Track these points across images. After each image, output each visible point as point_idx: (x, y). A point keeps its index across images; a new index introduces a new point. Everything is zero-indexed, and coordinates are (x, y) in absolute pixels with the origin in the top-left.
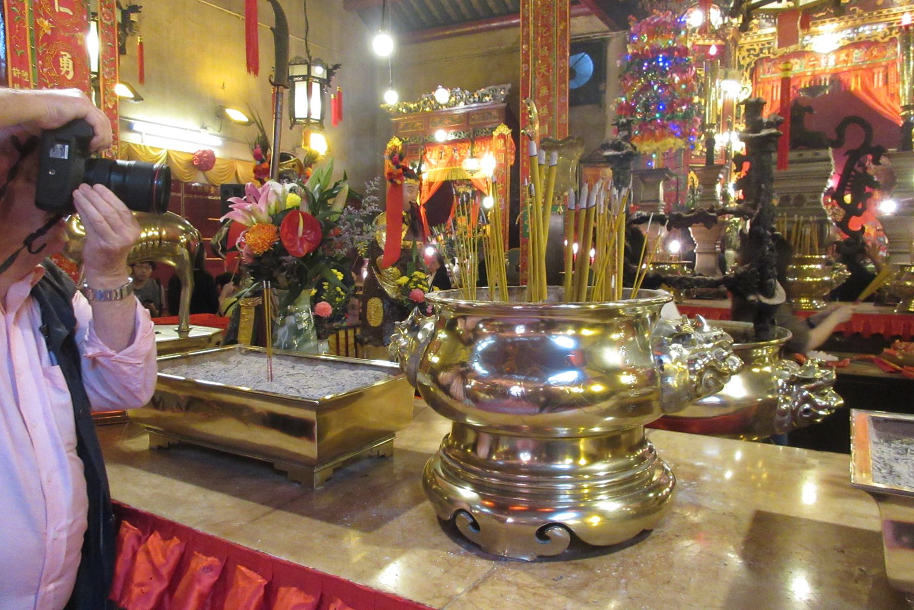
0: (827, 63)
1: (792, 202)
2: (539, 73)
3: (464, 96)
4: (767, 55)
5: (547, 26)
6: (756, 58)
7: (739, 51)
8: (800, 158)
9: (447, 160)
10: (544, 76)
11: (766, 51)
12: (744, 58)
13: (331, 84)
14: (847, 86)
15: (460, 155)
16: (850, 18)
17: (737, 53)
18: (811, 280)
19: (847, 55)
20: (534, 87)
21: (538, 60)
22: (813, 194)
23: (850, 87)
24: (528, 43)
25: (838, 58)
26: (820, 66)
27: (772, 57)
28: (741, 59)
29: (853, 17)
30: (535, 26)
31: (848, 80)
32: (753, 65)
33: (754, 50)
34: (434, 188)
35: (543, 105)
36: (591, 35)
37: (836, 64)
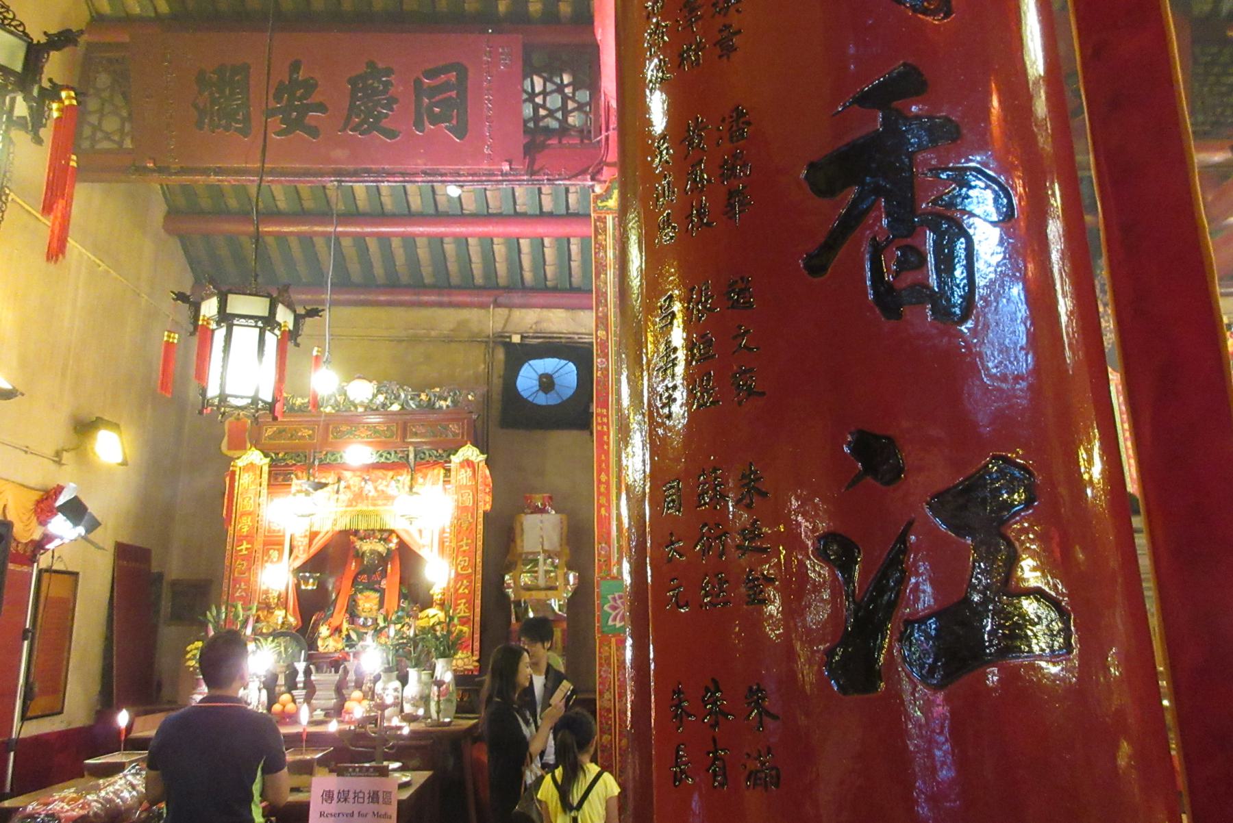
3: (403, 396)
9: (349, 495)
13: (299, 340)
15: (376, 488)
34: (318, 543)
36: (576, 337)
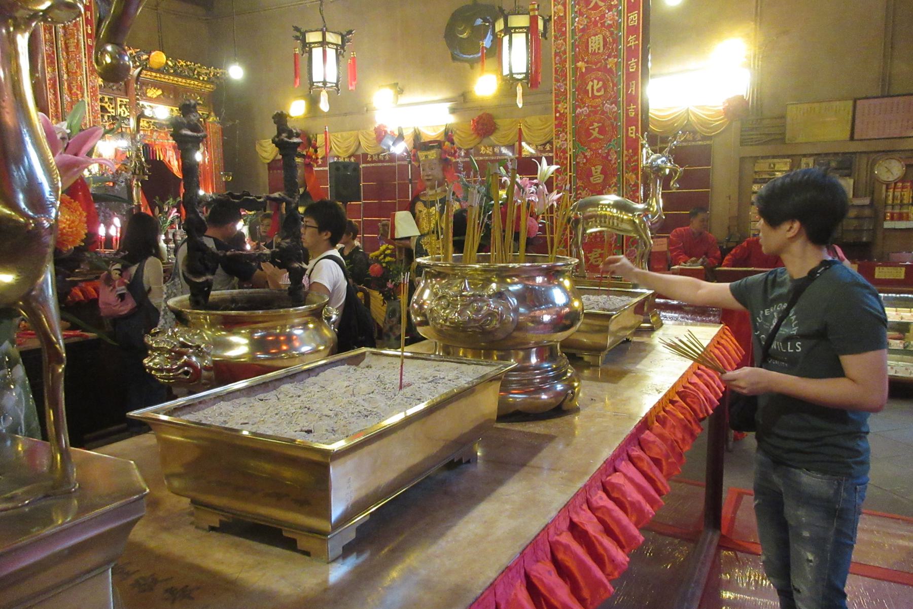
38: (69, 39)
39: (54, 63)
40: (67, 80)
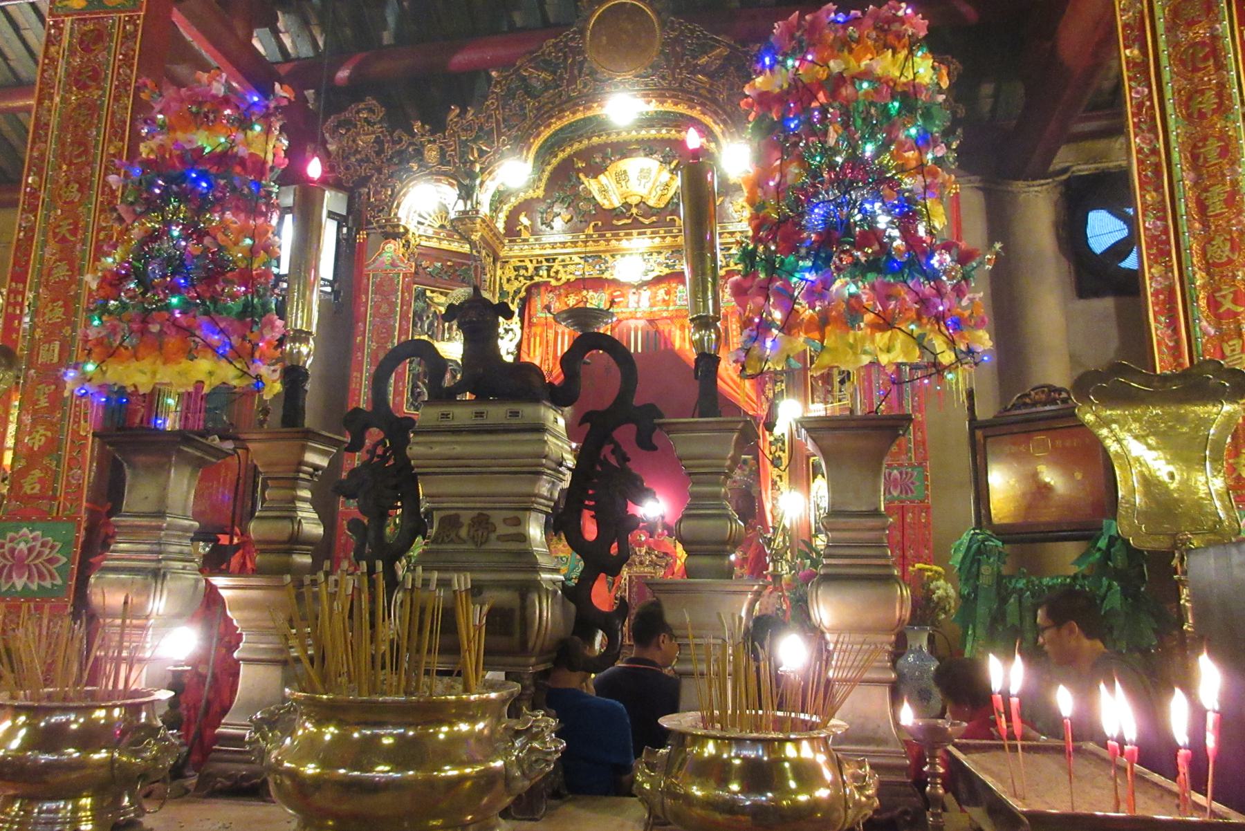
0: (638, 302)
1: (463, 532)
2: (55, 235)
4: (546, 279)
5: (82, 144)
6: (529, 283)
7: (502, 268)
8: (479, 421)
10: (63, 240)
11: (543, 273)
12: (509, 280)
14: (668, 341)
16: (665, 232)
17: (499, 272)
18: (455, 773)
19: (668, 293)
20: (42, 263)
21: (55, 208)
22: (511, 514)
23: (673, 345)
24: (39, 173)
25: (655, 295)
26: (627, 307)
27: (553, 282)
28: (504, 281)
29: (671, 232)
30: (61, 142)
31: (670, 331)
32: (523, 294)
33: (526, 269)
35: (53, 301)
37: (652, 306)
38: (1206, 190)
39: (1169, 254)
40: (1204, 287)
